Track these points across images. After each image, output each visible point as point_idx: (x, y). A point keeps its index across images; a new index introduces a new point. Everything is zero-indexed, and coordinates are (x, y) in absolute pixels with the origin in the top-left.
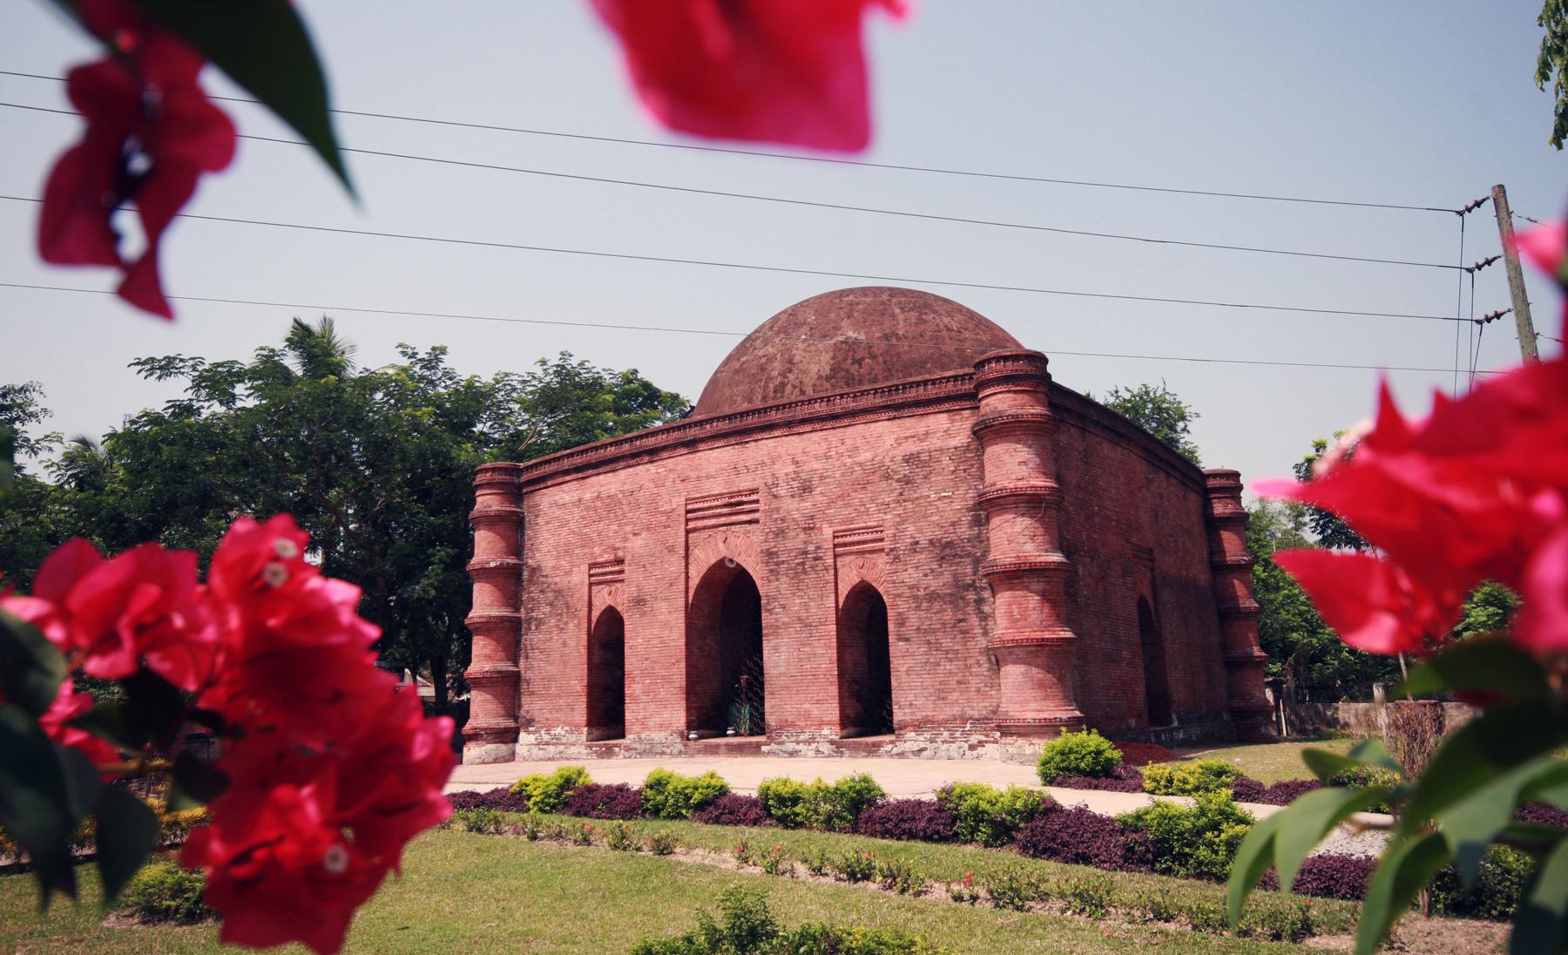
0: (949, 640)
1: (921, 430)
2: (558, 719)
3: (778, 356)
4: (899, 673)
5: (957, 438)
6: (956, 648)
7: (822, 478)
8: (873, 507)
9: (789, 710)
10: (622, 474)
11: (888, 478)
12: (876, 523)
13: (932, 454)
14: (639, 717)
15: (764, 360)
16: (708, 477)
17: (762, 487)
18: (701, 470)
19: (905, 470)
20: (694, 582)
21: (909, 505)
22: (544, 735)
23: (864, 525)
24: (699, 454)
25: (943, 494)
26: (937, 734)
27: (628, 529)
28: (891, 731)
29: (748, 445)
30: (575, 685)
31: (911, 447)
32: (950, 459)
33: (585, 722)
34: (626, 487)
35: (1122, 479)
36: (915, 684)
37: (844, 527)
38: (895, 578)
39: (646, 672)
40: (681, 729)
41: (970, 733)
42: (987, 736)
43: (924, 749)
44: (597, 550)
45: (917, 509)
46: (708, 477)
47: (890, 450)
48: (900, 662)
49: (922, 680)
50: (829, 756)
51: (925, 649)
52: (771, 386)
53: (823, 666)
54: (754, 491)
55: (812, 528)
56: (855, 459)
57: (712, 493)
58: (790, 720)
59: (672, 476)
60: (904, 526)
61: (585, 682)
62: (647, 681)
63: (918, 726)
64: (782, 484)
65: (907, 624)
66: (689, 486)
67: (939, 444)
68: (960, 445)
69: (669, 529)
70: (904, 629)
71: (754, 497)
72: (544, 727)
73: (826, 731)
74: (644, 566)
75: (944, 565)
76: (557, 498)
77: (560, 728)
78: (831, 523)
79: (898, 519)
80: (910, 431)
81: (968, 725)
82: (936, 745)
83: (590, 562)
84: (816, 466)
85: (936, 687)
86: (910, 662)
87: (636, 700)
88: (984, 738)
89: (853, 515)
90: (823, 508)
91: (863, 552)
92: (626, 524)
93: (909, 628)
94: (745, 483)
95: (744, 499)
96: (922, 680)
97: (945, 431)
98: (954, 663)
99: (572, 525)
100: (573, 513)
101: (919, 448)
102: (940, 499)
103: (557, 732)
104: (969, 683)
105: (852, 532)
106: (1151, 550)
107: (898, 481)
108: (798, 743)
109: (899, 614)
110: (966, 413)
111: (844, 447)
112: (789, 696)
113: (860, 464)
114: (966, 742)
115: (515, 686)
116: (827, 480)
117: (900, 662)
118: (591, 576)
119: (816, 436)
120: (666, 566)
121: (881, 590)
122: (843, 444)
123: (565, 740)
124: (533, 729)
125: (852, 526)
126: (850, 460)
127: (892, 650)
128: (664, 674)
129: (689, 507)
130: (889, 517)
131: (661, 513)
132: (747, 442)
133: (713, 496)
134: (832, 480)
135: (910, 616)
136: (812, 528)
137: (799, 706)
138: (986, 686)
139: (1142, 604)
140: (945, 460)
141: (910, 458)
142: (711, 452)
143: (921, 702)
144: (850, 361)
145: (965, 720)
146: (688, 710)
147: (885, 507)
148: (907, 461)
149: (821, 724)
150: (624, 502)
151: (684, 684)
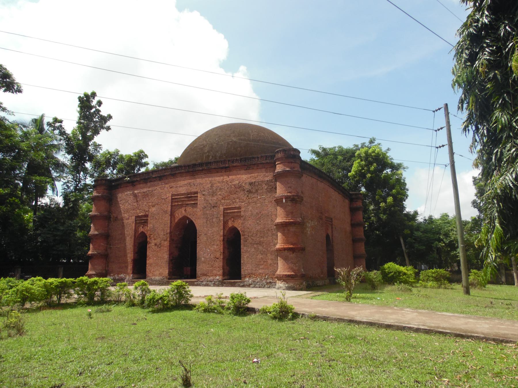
3: (208, 145)
5: (268, 178)
7: (220, 189)
8: (238, 200)
10: (149, 184)
11: (244, 190)
12: (238, 206)
13: (259, 183)
14: (151, 271)
15: (202, 146)
20: (174, 224)
21: (251, 200)
23: (234, 206)
24: (177, 179)
27: (150, 204)
28: (240, 278)
31: (253, 181)
32: (265, 185)
33: (131, 273)
35: (323, 194)
37: (227, 207)
40: (166, 275)
42: (273, 280)
43: (252, 284)
45: (253, 202)
48: (244, 254)
50: (218, 286)
52: (205, 156)
54: (196, 193)
55: (216, 207)
58: (205, 273)
59: (167, 186)
63: (250, 275)
65: (247, 241)
66: (173, 189)
67: (262, 179)
68: (269, 180)
69: (165, 205)
70: (246, 243)
71: (195, 195)
81: (267, 276)
82: (255, 283)
85: (256, 263)
86: (248, 255)
87: (151, 265)
92: (149, 202)
94: (194, 190)
95: (193, 195)
101: (255, 180)
103: (121, 276)
104: (267, 262)
106: (332, 219)
107: (247, 191)
109: (245, 238)
111: (229, 179)
113: (234, 185)
115: (106, 259)
118: (136, 220)
121: (239, 229)
125: (230, 207)
127: (242, 250)
129: (173, 197)
130: (243, 204)
131: (163, 199)
132: (195, 175)
133: (182, 193)
136: (216, 207)
137: (208, 269)
138: (273, 263)
139: (328, 236)
140: (264, 185)
142: (181, 178)
144: (233, 148)
146: (169, 269)
147: (242, 200)
148: (251, 185)
149: (216, 275)
150: (149, 194)
151: (168, 260)
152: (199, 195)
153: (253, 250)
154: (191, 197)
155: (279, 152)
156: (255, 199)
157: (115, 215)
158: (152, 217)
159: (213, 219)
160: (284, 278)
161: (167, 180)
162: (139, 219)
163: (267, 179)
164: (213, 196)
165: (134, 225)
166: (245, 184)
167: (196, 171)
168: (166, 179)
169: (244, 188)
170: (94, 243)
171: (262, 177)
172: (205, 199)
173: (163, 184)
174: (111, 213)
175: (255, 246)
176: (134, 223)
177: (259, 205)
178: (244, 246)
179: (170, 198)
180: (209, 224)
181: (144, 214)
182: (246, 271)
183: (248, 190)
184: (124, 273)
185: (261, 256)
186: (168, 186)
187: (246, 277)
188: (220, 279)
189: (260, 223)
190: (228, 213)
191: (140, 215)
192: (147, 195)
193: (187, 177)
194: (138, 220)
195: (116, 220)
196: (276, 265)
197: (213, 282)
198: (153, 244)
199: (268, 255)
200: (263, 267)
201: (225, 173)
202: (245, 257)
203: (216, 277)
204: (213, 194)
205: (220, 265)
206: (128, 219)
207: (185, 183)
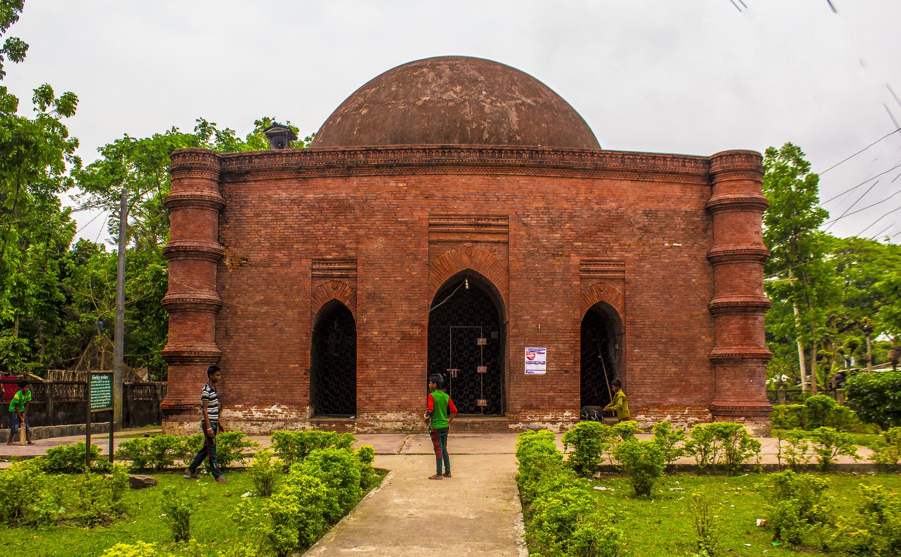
0: (675, 350)
1: (659, 193)
2: (272, 398)
4: (634, 372)
5: (688, 205)
6: (680, 356)
8: (616, 246)
9: (533, 397)
10: (354, 182)
14: (372, 399)
16: (455, 198)
17: (512, 214)
18: (448, 191)
19: (644, 221)
22: (254, 412)
23: (607, 258)
24: (445, 177)
25: (674, 244)
26: (662, 417)
29: (499, 178)
30: (295, 368)
31: (653, 206)
34: (359, 194)
36: (647, 380)
37: (590, 258)
38: (633, 301)
39: (381, 360)
41: (687, 416)
42: (699, 418)
44: (322, 248)
45: (653, 252)
46: (455, 198)
47: (633, 204)
49: (651, 378)
51: (657, 356)
53: (567, 364)
54: (506, 218)
55: (561, 255)
56: (602, 206)
57: (459, 213)
59: (414, 192)
60: (642, 264)
61: (309, 365)
62: (383, 369)
64: (533, 216)
68: (689, 210)
70: (640, 340)
72: (254, 405)
73: (567, 414)
74: (381, 268)
75: (674, 296)
76: (270, 193)
77: (275, 406)
78: (578, 254)
79: (637, 258)
80: (650, 193)
81: (687, 410)
83: (314, 257)
84: (566, 206)
86: (644, 364)
88: (698, 420)
89: (598, 250)
90: (571, 241)
91: (605, 278)
93: (645, 340)
95: (492, 222)
96: (651, 378)
97: (678, 198)
98: (678, 367)
99: (289, 220)
100: (291, 209)
102: (671, 247)
103: (271, 410)
105: (595, 262)
108: (544, 422)
110: (696, 188)
111: (591, 195)
112: (535, 386)
114: (686, 422)
116: (576, 219)
117: (635, 364)
119: (564, 182)
120: (408, 270)
122: (591, 192)
123: (281, 417)
124: (240, 406)
126: (599, 206)
128: (402, 363)
133: (459, 215)
134: (580, 219)
135: (645, 331)
137: (543, 394)
140: (678, 220)
141: (649, 213)
143: (651, 394)
145: (685, 407)
147: (626, 247)
149: (563, 408)
152: (512, 224)
153: (655, 355)
154: (486, 225)
155: (724, 158)
156: (657, 246)
157: (238, 252)
158: (371, 265)
159: (553, 282)
160: (749, 414)
161: (413, 177)
162: (322, 266)
163: (685, 208)
164: (552, 231)
165: (308, 282)
166: (634, 212)
167: (503, 166)
168: (413, 174)
169: (632, 220)
170: (189, 323)
171: (672, 203)
172: (530, 235)
173: (401, 185)
174: (223, 245)
175: (661, 347)
176: (310, 276)
177: (667, 261)
178: (635, 345)
179: (425, 224)
180: (541, 293)
181: (342, 256)
182: (639, 399)
183: (641, 226)
184: (282, 402)
185: (674, 370)
186: (419, 193)
187: (638, 411)
188: (574, 417)
189: (672, 299)
190: (589, 271)
191: (328, 257)
192: (350, 208)
193: (474, 177)
194: (319, 270)
195: (241, 265)
196: (706, 388)
197: (560, 424)
198: (376, 333)
199: (691, 368)
200: (678, 391)
201: (581, 181)
202: (637, 370)
203: (565, 412)
204: (552, 226)
205: (574, 386)
206: (289, 264)
207: (471, 191)
